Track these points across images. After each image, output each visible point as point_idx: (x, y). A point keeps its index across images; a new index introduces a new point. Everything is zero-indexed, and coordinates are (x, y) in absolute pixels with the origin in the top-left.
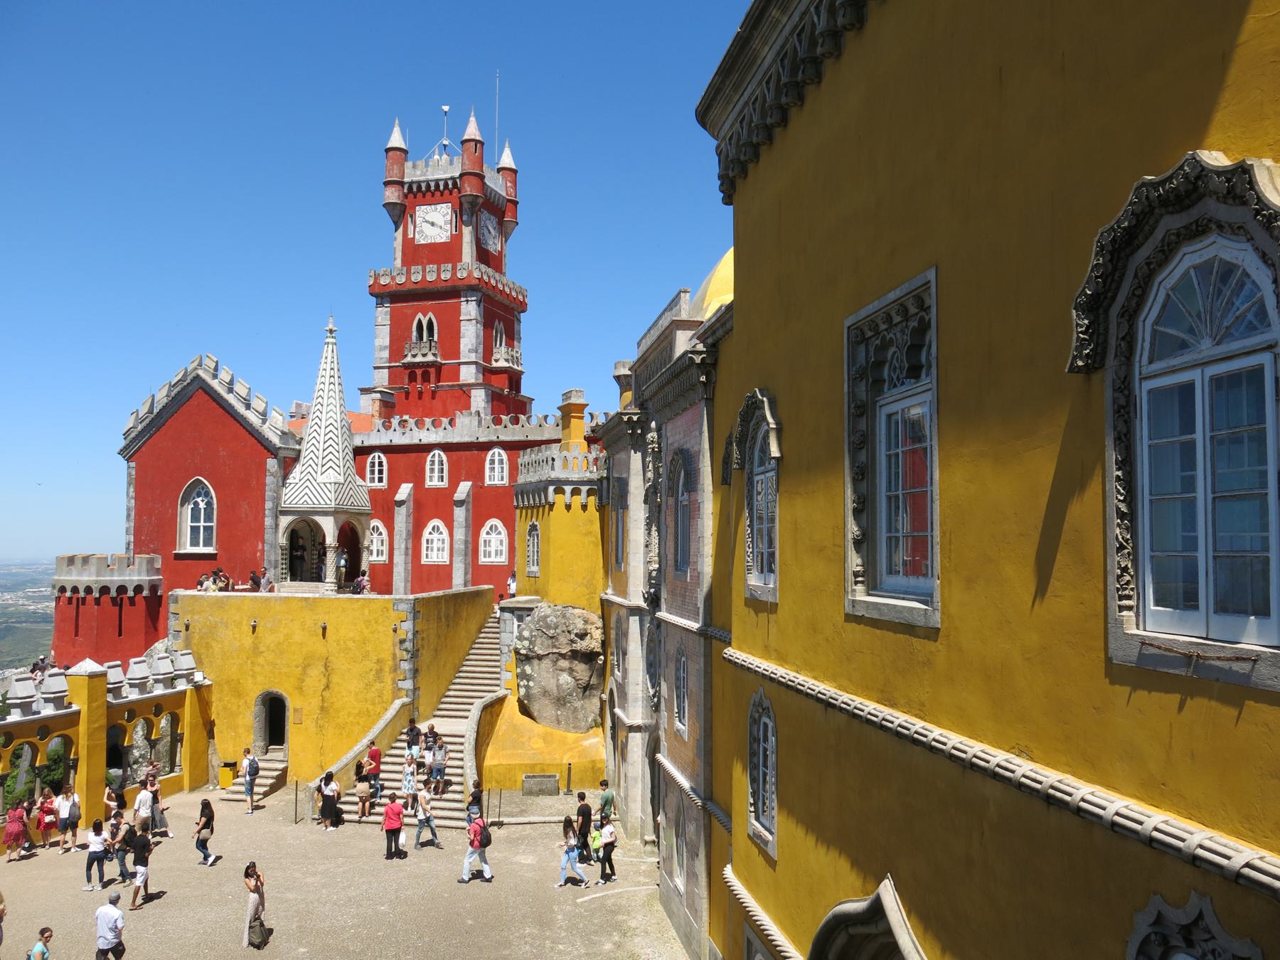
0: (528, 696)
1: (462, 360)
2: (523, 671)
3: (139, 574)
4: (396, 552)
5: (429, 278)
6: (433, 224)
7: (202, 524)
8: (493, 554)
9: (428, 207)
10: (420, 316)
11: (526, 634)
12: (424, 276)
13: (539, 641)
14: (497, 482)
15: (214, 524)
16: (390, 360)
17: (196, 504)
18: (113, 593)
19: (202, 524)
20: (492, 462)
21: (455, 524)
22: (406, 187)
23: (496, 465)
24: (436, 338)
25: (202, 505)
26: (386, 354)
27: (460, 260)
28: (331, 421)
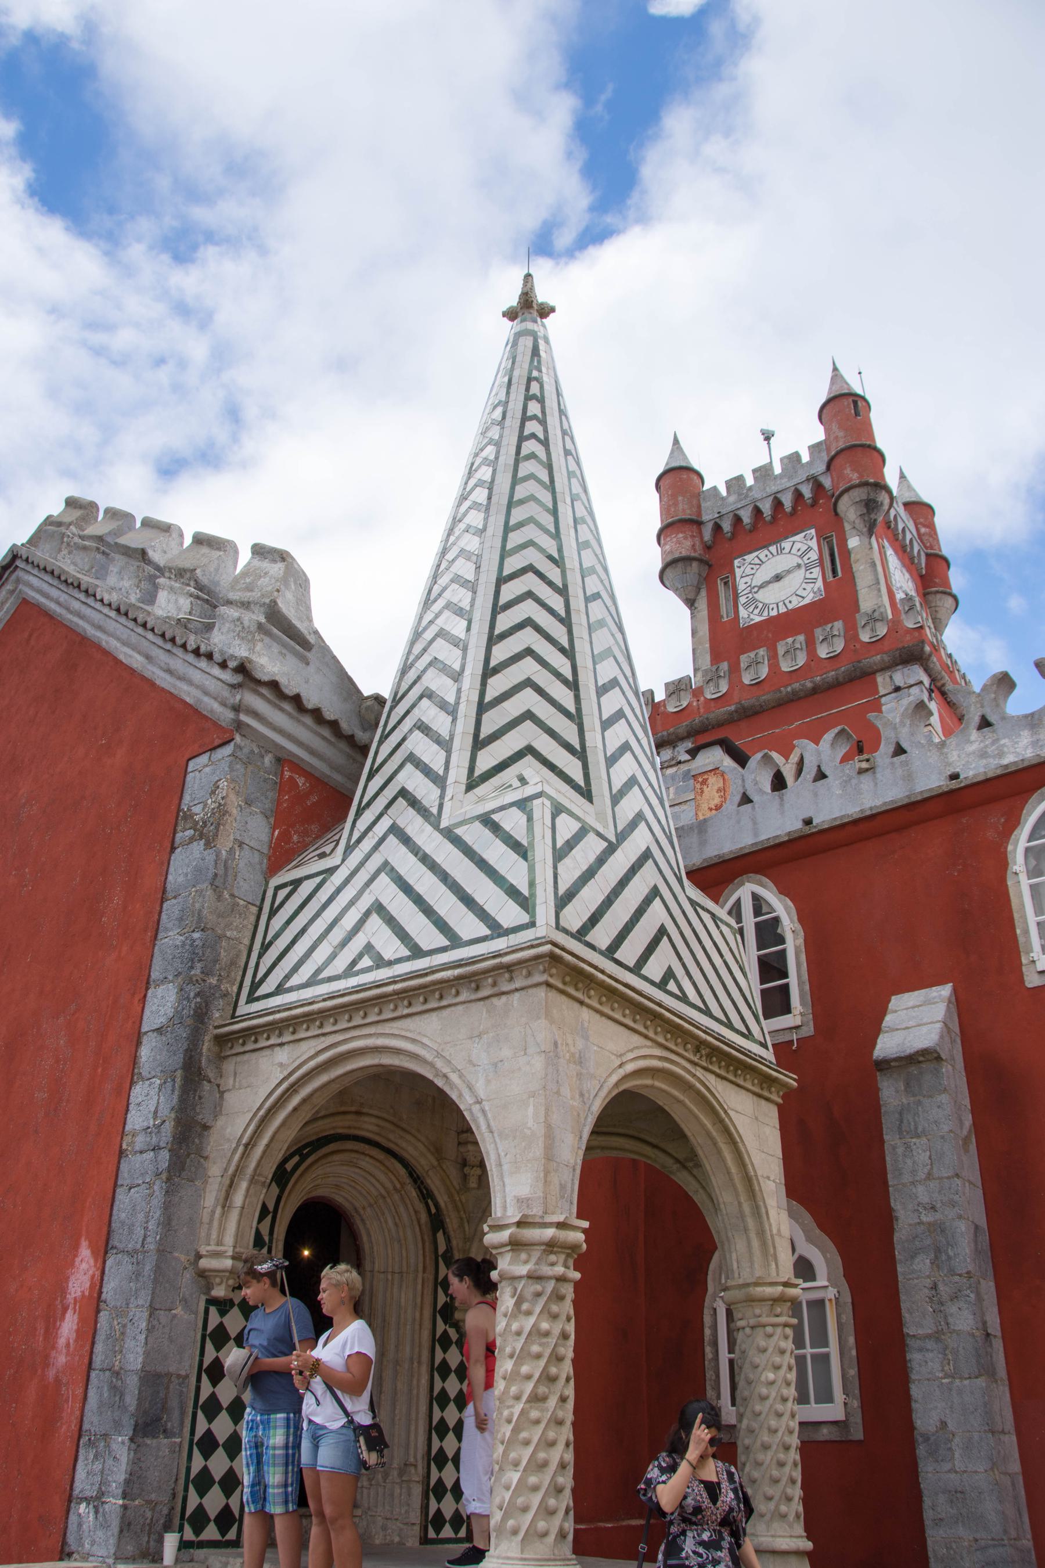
5: (785, 667)
6: (778, 578)
9: (763, 554)
12: (774, 666)
22: (707, 533)
27: (857, 608)
28: (530, 556)
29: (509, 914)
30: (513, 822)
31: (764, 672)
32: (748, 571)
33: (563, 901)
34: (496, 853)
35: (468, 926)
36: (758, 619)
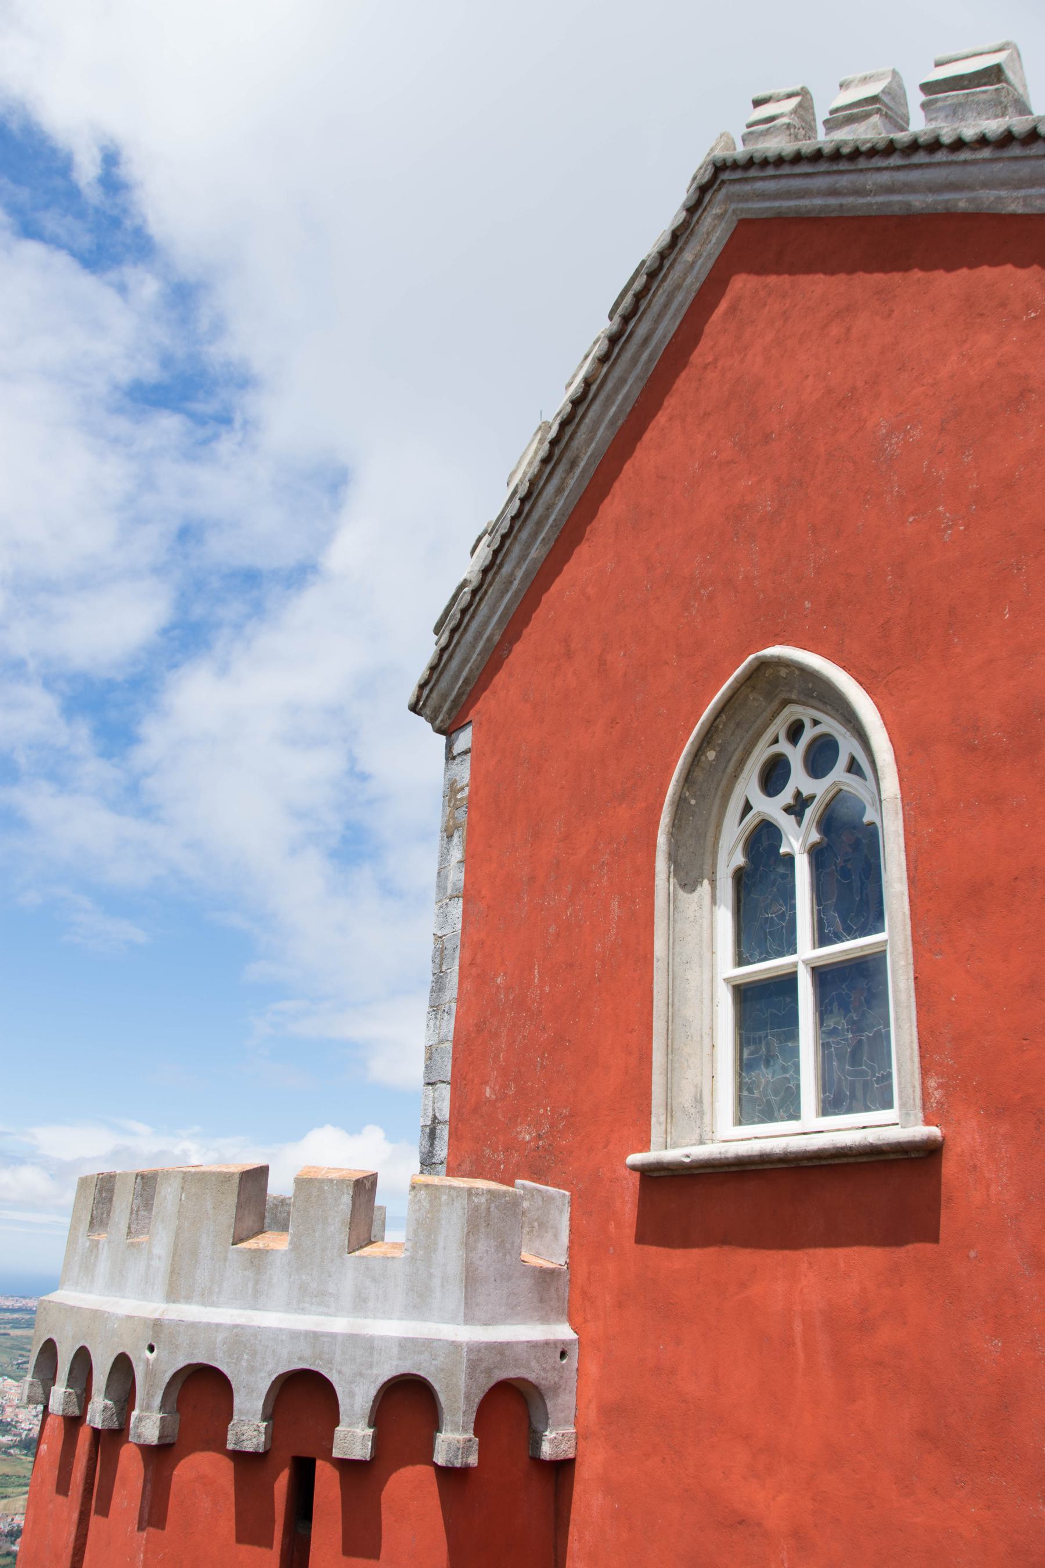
3: (419, 1300)
15: (894, 938)
17: (763, 840)
18: (249, 1427)
19: (806, 952)
25: (797, 841)
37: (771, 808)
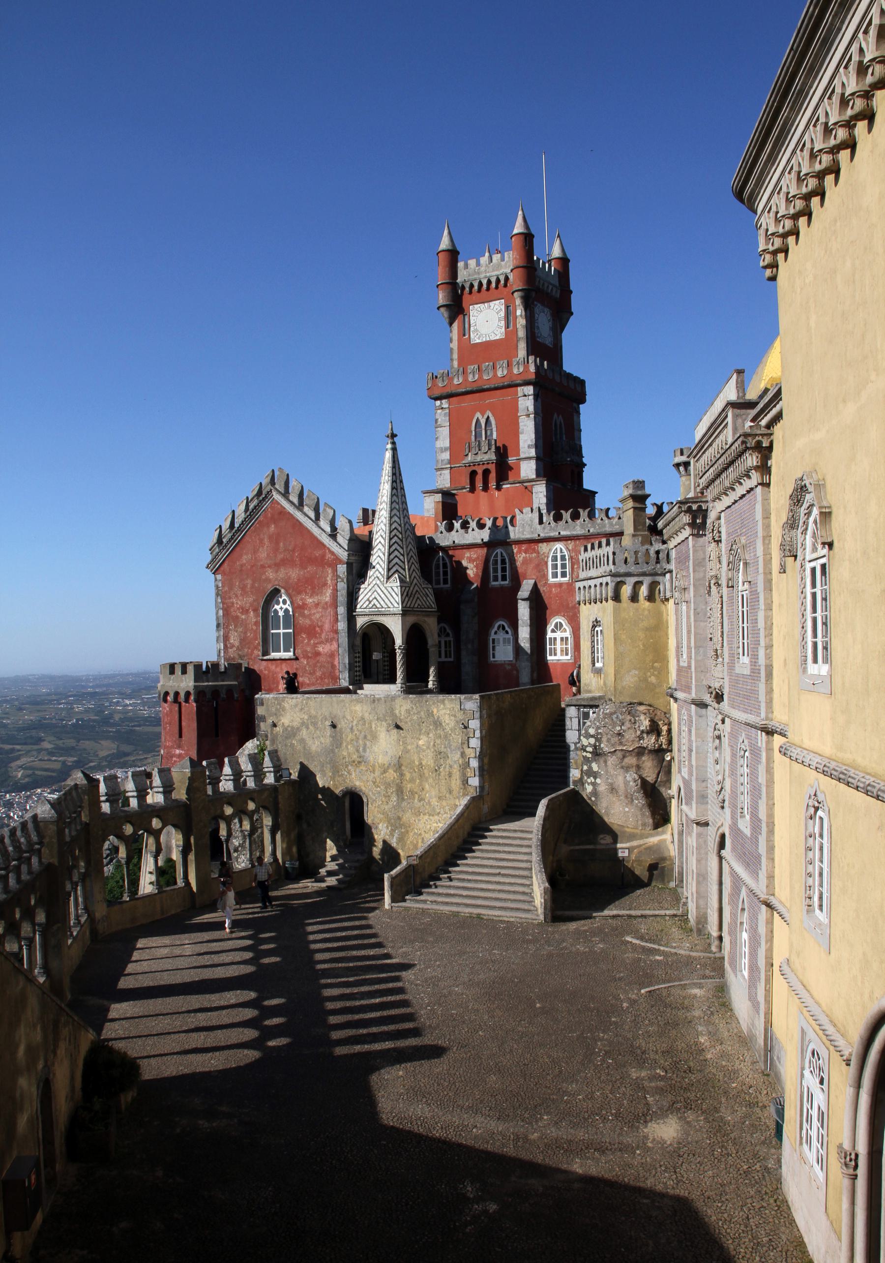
0: (595, 793)
1: (522, 456)
2: (590, 768)
4: (464, 653)
7: (281, 631)
8: (559, 652)
9: (482, 306)
10: (478, 415)
11: (592, 731)
13: (604, 739)
14: (559, 579)
16: (450, 462)
17: (276, 611)
20: (555, 559)
21: (520, 622)
23: (559, 563)
24: (495, 436)
25: (281, 613)
26: (446, 456)
29: (396, 605)
30: (395, 589)
31: (477, 377)
32: (475, 314)
33: (402, 603)
34: (393, 594)
35: (390, 605)
36: (478, 341)
37: (276, 607)
